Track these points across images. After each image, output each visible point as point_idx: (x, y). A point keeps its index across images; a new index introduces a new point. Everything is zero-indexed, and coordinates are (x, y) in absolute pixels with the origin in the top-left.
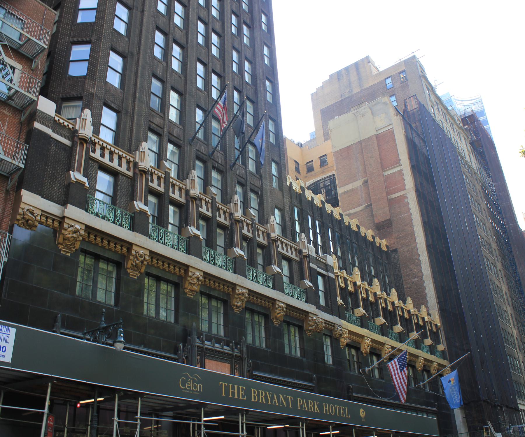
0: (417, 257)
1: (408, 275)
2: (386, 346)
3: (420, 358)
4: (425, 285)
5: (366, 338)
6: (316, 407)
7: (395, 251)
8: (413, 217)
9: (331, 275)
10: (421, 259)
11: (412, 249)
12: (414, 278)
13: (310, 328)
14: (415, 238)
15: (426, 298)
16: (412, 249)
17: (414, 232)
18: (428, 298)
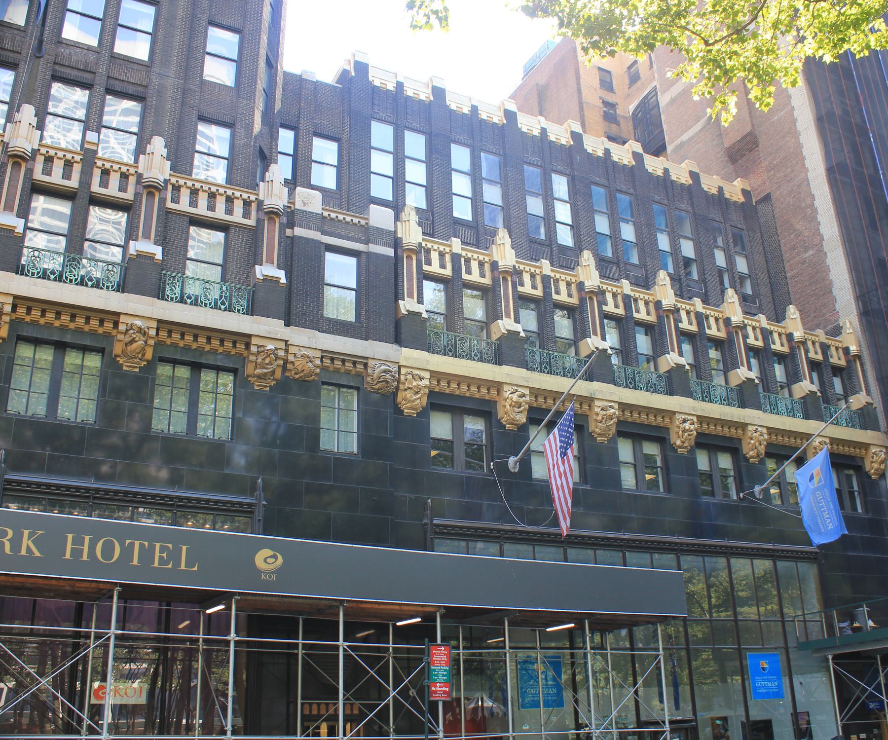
0: (809, 202)
1: (793, 248)
2: (597, 403)
3: (750, 428)
4: (829, 261)
5: (506, 388)
6: (26, 542)
7: (767, 198)
8: (796, 113)
9: (375, 248)
10: (816, 203)
11: (799, 186)
12: (806, 250)
13: (258, 371)
14: (804, 159)
15: (831, 292)
16: (799, 186)
17: (799, 146)
18: (835, 292)
